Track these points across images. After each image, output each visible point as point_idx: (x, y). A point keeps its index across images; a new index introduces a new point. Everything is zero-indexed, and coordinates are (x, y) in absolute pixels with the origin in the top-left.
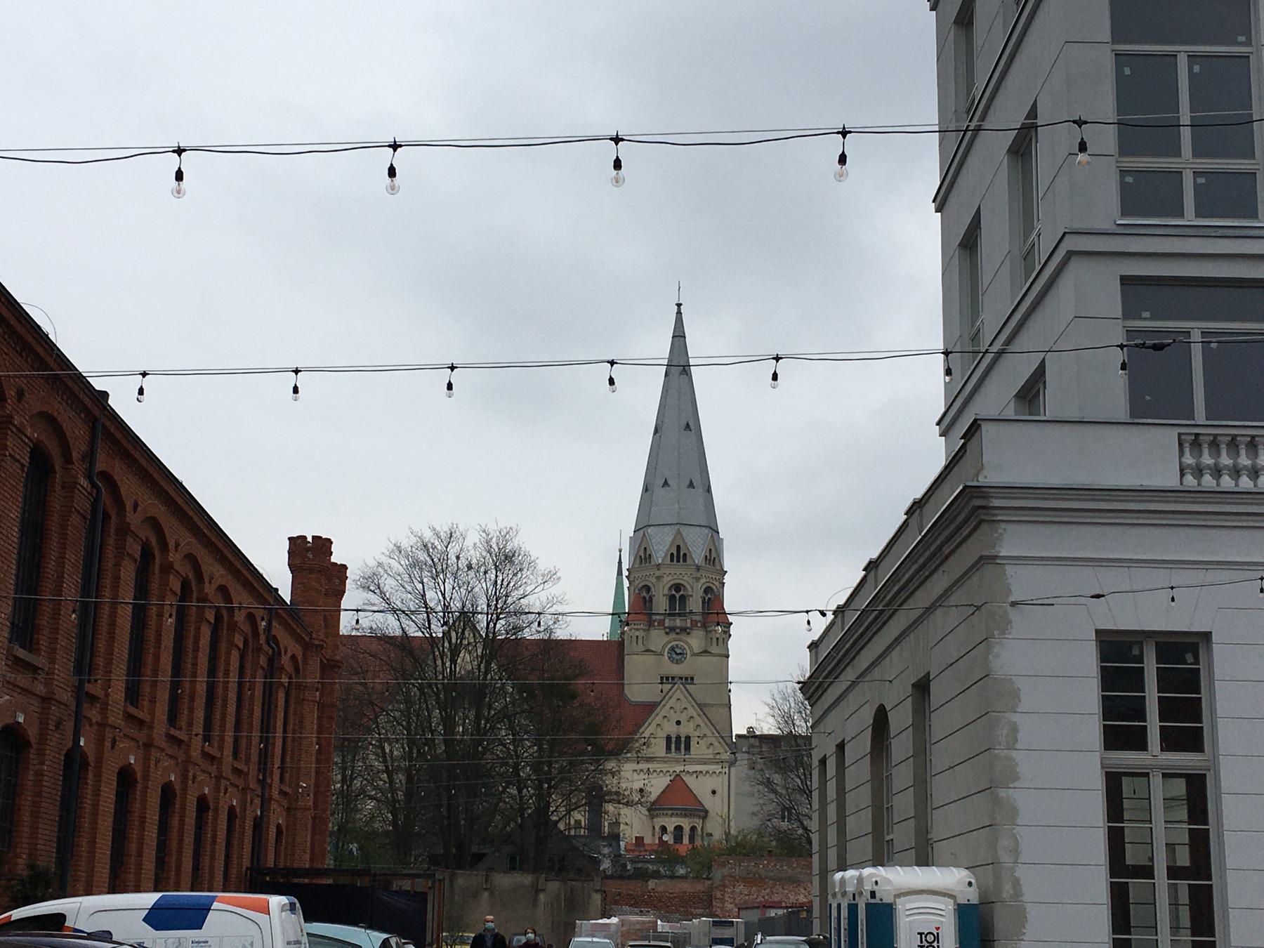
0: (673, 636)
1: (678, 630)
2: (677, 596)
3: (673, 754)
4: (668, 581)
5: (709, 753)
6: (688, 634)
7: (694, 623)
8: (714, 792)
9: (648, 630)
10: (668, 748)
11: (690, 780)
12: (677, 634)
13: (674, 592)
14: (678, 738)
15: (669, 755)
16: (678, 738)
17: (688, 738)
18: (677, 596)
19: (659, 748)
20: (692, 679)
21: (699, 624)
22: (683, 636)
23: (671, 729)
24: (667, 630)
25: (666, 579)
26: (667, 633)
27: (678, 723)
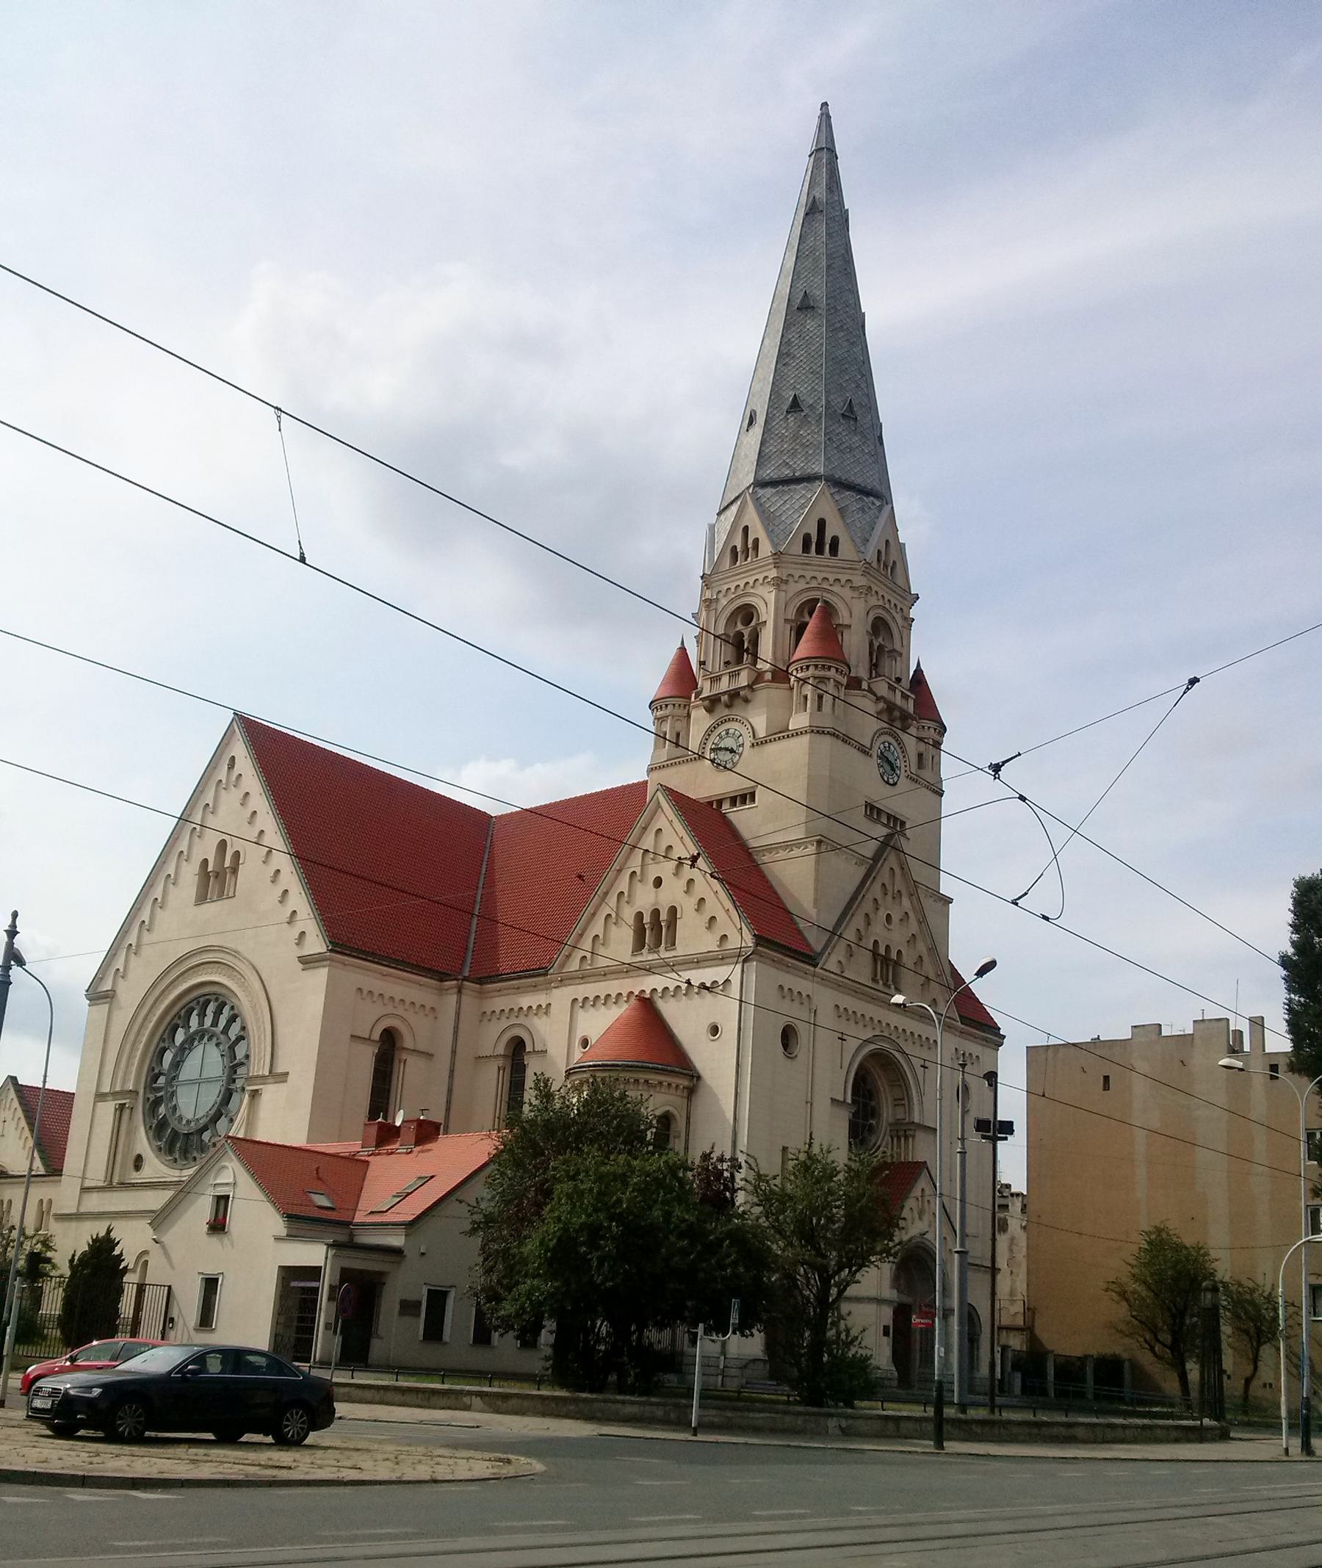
0: (721, 712)
1: (725, 698)
2: (746, 632)
3: (646, 956)
4: (726, 605)
5: (709, 943)
6: (747, 701)
7: (759, 677)
8: (715, 1030)
9: (689, 716)
10: (639, 944)
11: (668, 1009)
12: (728, 706)
13: (740, 627)
14: (656, 913)
15: (639, 959)
16: (656, 913)
17: (673, 910)
18: (746, 632)
19: (620, 945)
20: (753, 795)
21: (768, 676)
22: (737, 711)
23: (645, 899)
24: (707, 703)
25: (724, 602)
26: (710, 710)
27: (658, 882)
